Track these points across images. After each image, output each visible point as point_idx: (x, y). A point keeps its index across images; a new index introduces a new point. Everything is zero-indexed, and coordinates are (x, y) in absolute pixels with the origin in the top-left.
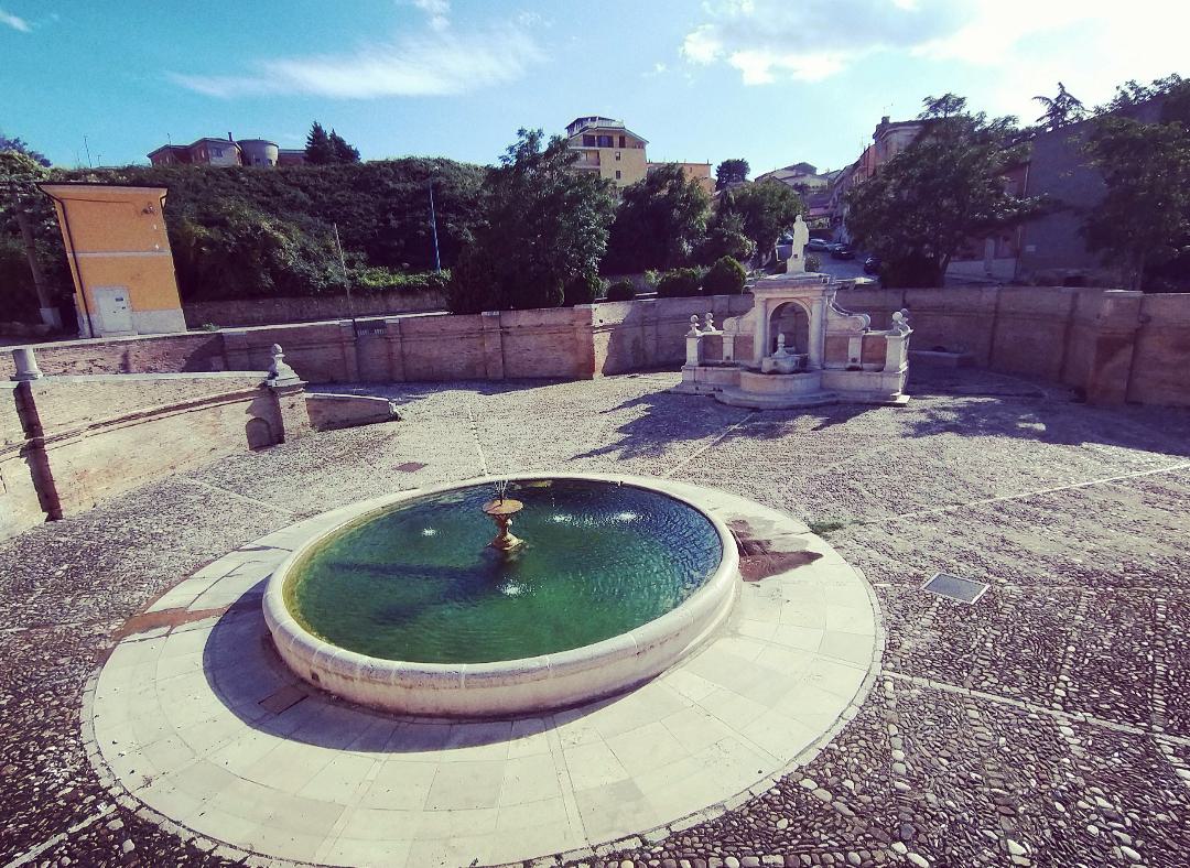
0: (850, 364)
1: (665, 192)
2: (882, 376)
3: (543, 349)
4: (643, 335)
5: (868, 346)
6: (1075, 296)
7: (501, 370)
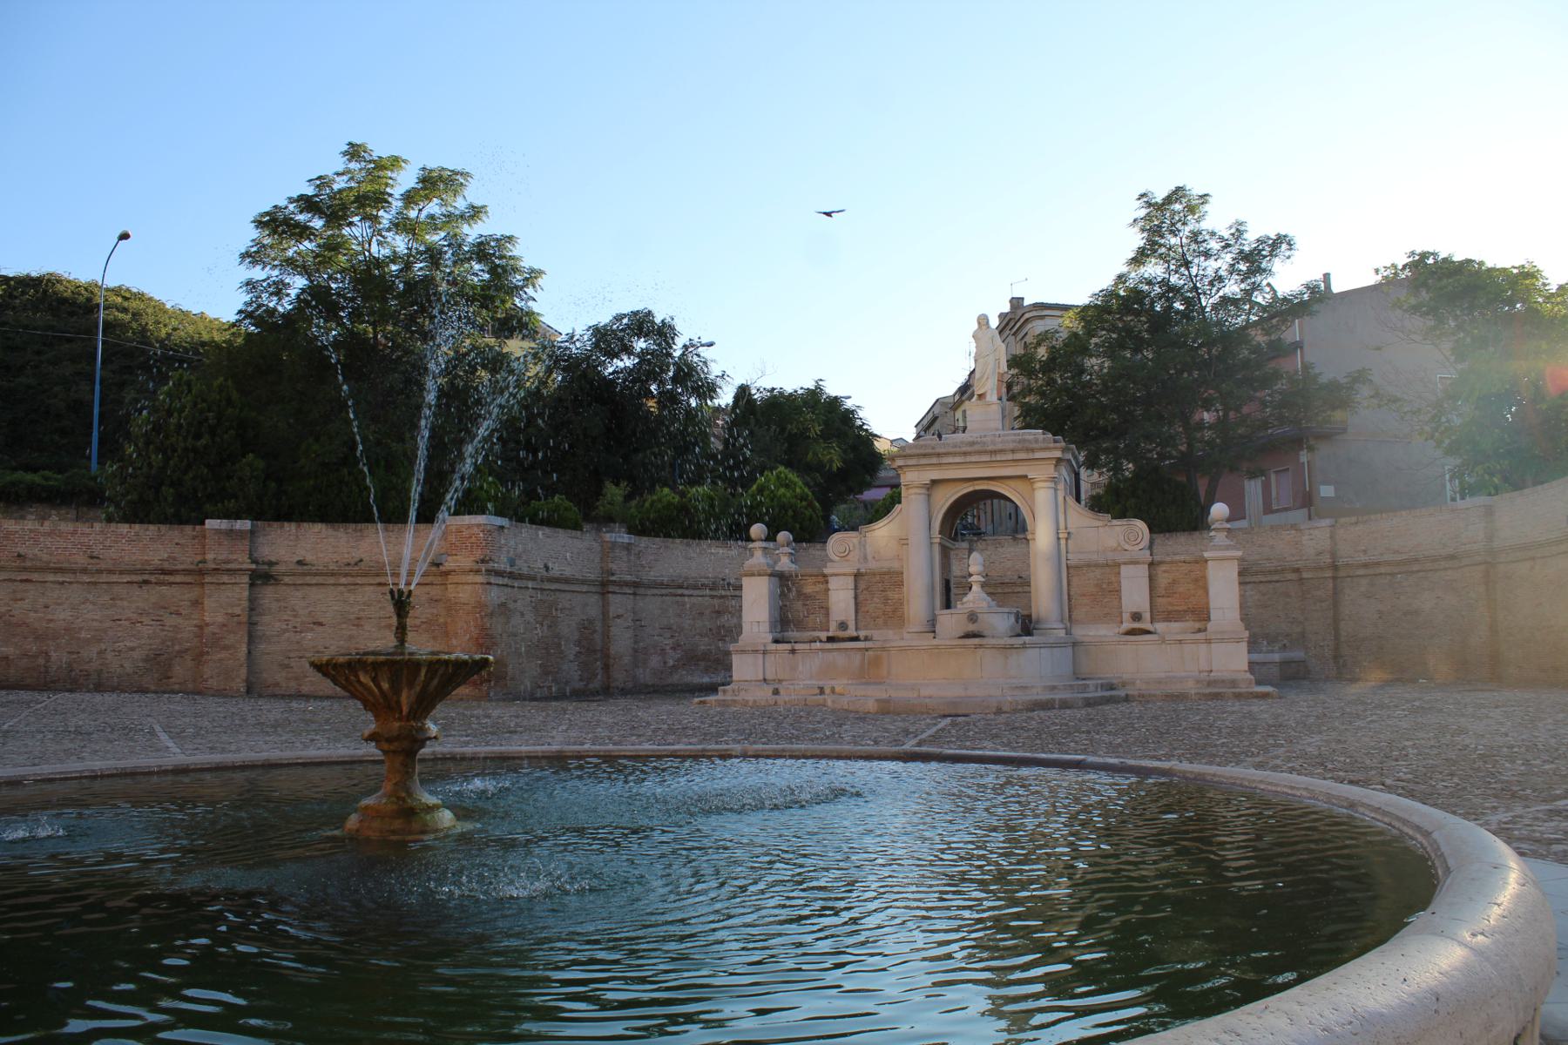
0: (1128, 625)
1: (627, 362)
3: (358, 622)
4: (605, 614)
5: (1163, 580)
6: (1489, 512)
7: (243, 672)
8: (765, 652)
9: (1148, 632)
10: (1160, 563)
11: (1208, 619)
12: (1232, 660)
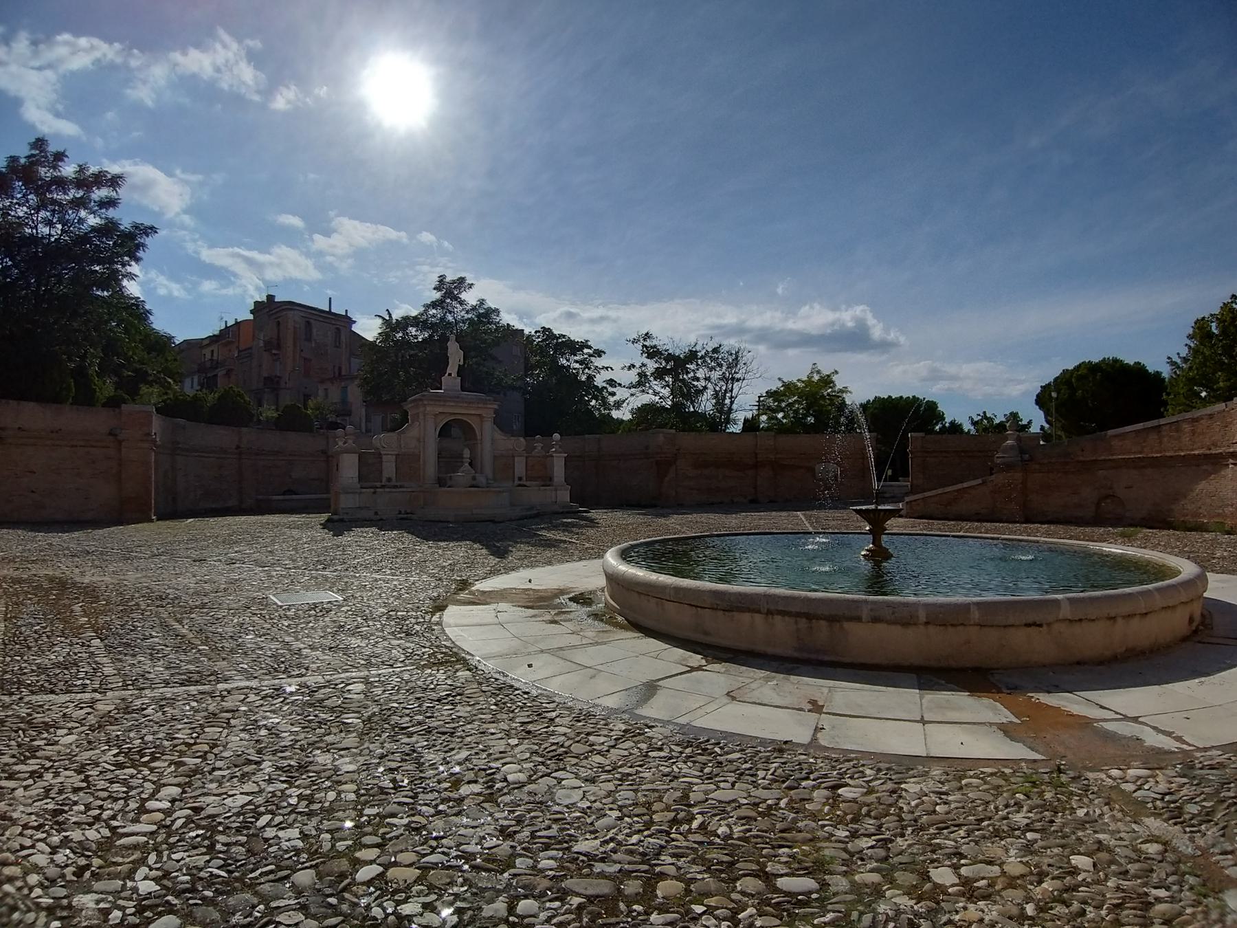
0: (517, 482)
2: (556, 490)
8: (361, 493)
9: (525, 486)
10: (529, 456)
11: (551, 479)
12: (565, 496)
